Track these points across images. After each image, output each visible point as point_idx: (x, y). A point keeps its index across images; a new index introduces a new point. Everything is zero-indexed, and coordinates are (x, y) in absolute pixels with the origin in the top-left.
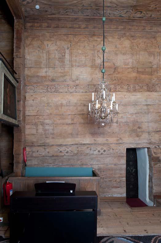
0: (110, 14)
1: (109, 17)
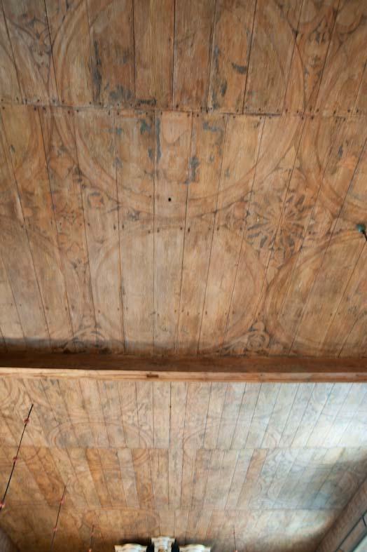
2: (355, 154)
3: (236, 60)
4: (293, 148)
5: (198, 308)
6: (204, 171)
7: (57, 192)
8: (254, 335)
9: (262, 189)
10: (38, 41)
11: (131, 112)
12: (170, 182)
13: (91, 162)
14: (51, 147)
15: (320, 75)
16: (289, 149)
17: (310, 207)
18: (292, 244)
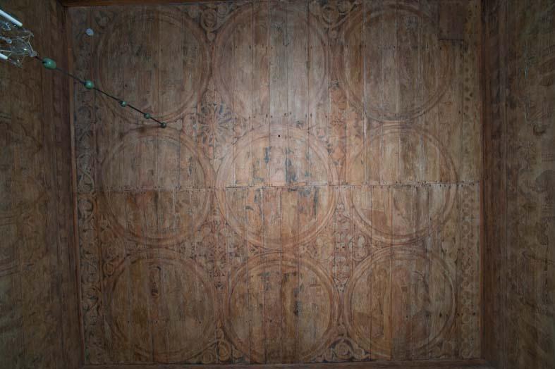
0: (82, 157)
1: (76, 158)
2: (183, 170)
3: (252, 211)
4: (216, 170)
5: (256, 51)
6: (261, 155)
7: (343, 138)
8: (213, 27)
9: (228, 146)
10: (340, 213)
11: (300, 185)
12: (279, 148)
13: (322, 157)
14: (342, 164)
15: (212, 208)
17: (198, 136)
18: (203, 109)
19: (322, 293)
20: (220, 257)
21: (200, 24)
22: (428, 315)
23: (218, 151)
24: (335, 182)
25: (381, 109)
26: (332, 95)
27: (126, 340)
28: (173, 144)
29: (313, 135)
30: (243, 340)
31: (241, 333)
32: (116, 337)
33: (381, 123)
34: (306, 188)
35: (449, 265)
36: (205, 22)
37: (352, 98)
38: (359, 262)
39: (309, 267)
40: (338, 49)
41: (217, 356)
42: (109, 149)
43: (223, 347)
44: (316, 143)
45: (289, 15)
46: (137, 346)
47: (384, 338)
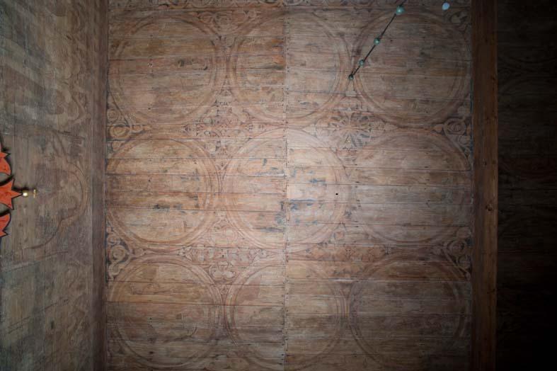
2: (305, 95)
4: (304, 129)
6: (318, 176)
7: (333, 257)
9: (328, 142)
11: (287, 214)
12: (325, 194)
14: (307, 257)
15: (266, 124)
16: (303, 131)
17: (339, 112)
18: (366, 118)
19: (178, 234)
20: (216, 131)
21: (451, 119)
22: (152, 340)
23: (323, 132)
24: (290, 249)
25: (360, 297)
26: (377, 248)
27: (133, 33)
28: (332, 87)
29: (337, 228)
30: (130, 152)
31: (138, 150)
32: (136, 22)
33: (348, 297)
34: (284, 220)
35: (201, 363)
36: (453, 122)
37: (374, 268)
38: (208, 272)
39: (204, 221)
40: (422, 255)
41: (115, 125)
42: (327, 22)
43: (124, 132)
44: (330, 230)
45: (457, 207)
46: (126, 44)
47: (129, 295)
